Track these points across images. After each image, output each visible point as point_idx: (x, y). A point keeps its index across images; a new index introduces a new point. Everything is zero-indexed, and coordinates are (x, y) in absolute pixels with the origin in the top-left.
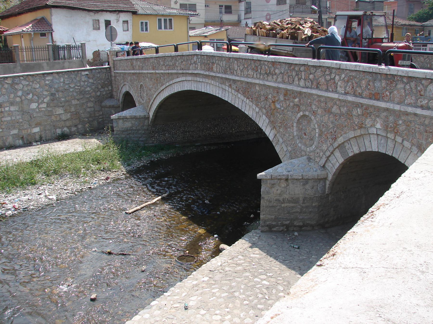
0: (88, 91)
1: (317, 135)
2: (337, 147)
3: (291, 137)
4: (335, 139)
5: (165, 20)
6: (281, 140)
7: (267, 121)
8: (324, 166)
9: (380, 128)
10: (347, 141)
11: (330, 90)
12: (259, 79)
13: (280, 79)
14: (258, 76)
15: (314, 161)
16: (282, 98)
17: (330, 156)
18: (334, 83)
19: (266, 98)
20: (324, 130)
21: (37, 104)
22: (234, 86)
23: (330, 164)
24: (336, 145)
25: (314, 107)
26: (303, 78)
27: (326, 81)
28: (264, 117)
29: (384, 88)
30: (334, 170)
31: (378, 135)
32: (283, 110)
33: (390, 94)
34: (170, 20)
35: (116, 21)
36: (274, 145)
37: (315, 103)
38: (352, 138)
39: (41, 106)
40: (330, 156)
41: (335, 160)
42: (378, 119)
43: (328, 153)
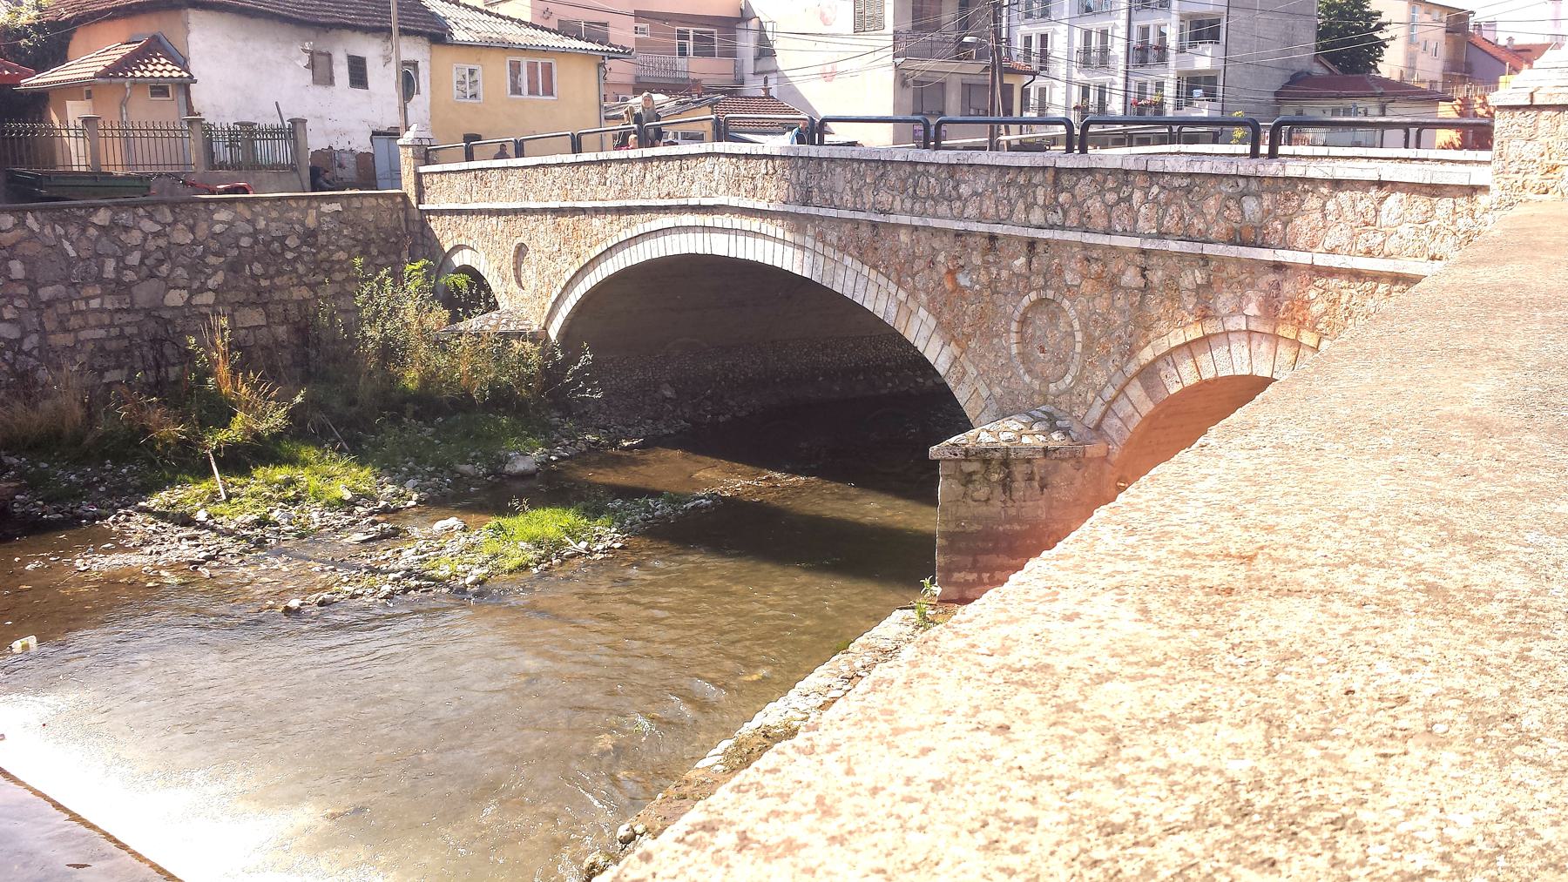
0: (339, 261)
1: (1078, 348)
2: (1138, 375)
3: (1002, 361)
4: (1131, 353)
5: (532, 68)
6: (972, 370)
7: (932, 322)
8: (1098, 427)
9: (1257, 313)
10: (1163, 356)
11: (1118, 228)
12: (912, 212)
13: (971, 211)
14: (908, 204)
15: (1070, 414)
16: (977, 260)
17: (1114, 400)
18: (1130, 208)
19: (932, 263)
20: (1097, 333)
21: (185, 293)
22: (832, 237)
23: (1116, 421)
24: (1133, 368)
25: (1069, 277)
26: (1040, 202)
27: (1107, 205)
28: (923, 313)
29: (1269, 212)
30: (1128, 435)
31: (1250, 332)
32: (980, 292)
33: (1285, 225)
34: (548, 69)
35: (381, 61)
36: (951, 385)
37: (1073, 265)
38: (1178, 347)
39: (198, 300)
40: (1114, 400)
41: (1130, 408)
42: (1250, 293)
43: (1110, 392)
